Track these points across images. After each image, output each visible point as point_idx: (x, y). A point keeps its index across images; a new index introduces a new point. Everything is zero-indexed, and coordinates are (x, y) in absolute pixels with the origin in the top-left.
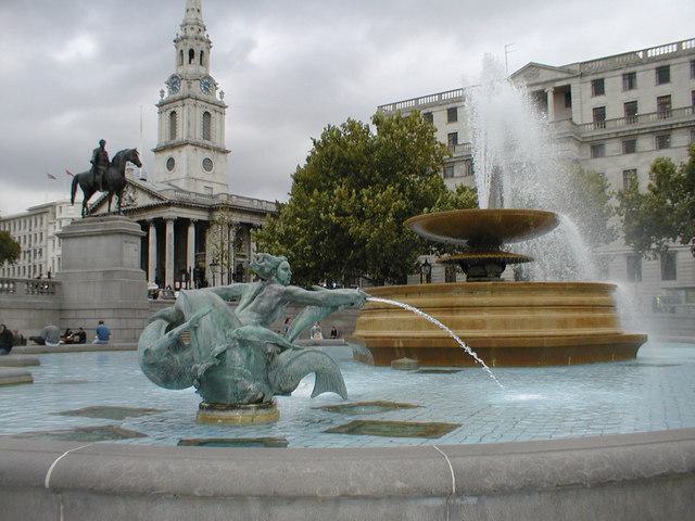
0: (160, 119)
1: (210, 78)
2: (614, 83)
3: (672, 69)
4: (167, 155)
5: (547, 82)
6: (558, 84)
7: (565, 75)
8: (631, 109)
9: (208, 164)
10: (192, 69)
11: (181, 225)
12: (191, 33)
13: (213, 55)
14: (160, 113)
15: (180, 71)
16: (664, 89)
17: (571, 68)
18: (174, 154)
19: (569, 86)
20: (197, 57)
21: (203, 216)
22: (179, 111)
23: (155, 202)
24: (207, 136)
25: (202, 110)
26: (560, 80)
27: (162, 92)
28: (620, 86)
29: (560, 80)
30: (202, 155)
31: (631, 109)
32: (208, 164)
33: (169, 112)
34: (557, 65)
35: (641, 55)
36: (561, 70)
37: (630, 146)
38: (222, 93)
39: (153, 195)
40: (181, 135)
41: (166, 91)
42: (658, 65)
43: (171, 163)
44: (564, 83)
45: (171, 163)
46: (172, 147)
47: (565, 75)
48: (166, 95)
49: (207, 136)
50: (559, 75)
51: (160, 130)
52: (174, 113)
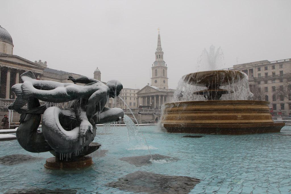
0: (152, 71)
1: (164, 62)
2: (263, 68)
3: (268, 67)
4: (155, 79)
5: (248, 68)
6: (250, 68)
7: (251, 67)
10: (160, 60)
11: (162, 96)
13: (164, 56)
14: (152, 69)
16: (266, 71)
19: (253, 69)
21: (165, 94)
22: (158, 69)
24: (164, 75)
25: (162, 69)
27: (153, 65)
30: (163, 79)
37: (266, 82)
38: (166, 65)
42: (273, 65)
43: (156, 82)
44: (251, 68)
45: (156, 82)
46: (157, 78)
47: (251, 67)
48: (154, 66)
49: (164, 75)
50: (250, 66)
51: (153, 73)
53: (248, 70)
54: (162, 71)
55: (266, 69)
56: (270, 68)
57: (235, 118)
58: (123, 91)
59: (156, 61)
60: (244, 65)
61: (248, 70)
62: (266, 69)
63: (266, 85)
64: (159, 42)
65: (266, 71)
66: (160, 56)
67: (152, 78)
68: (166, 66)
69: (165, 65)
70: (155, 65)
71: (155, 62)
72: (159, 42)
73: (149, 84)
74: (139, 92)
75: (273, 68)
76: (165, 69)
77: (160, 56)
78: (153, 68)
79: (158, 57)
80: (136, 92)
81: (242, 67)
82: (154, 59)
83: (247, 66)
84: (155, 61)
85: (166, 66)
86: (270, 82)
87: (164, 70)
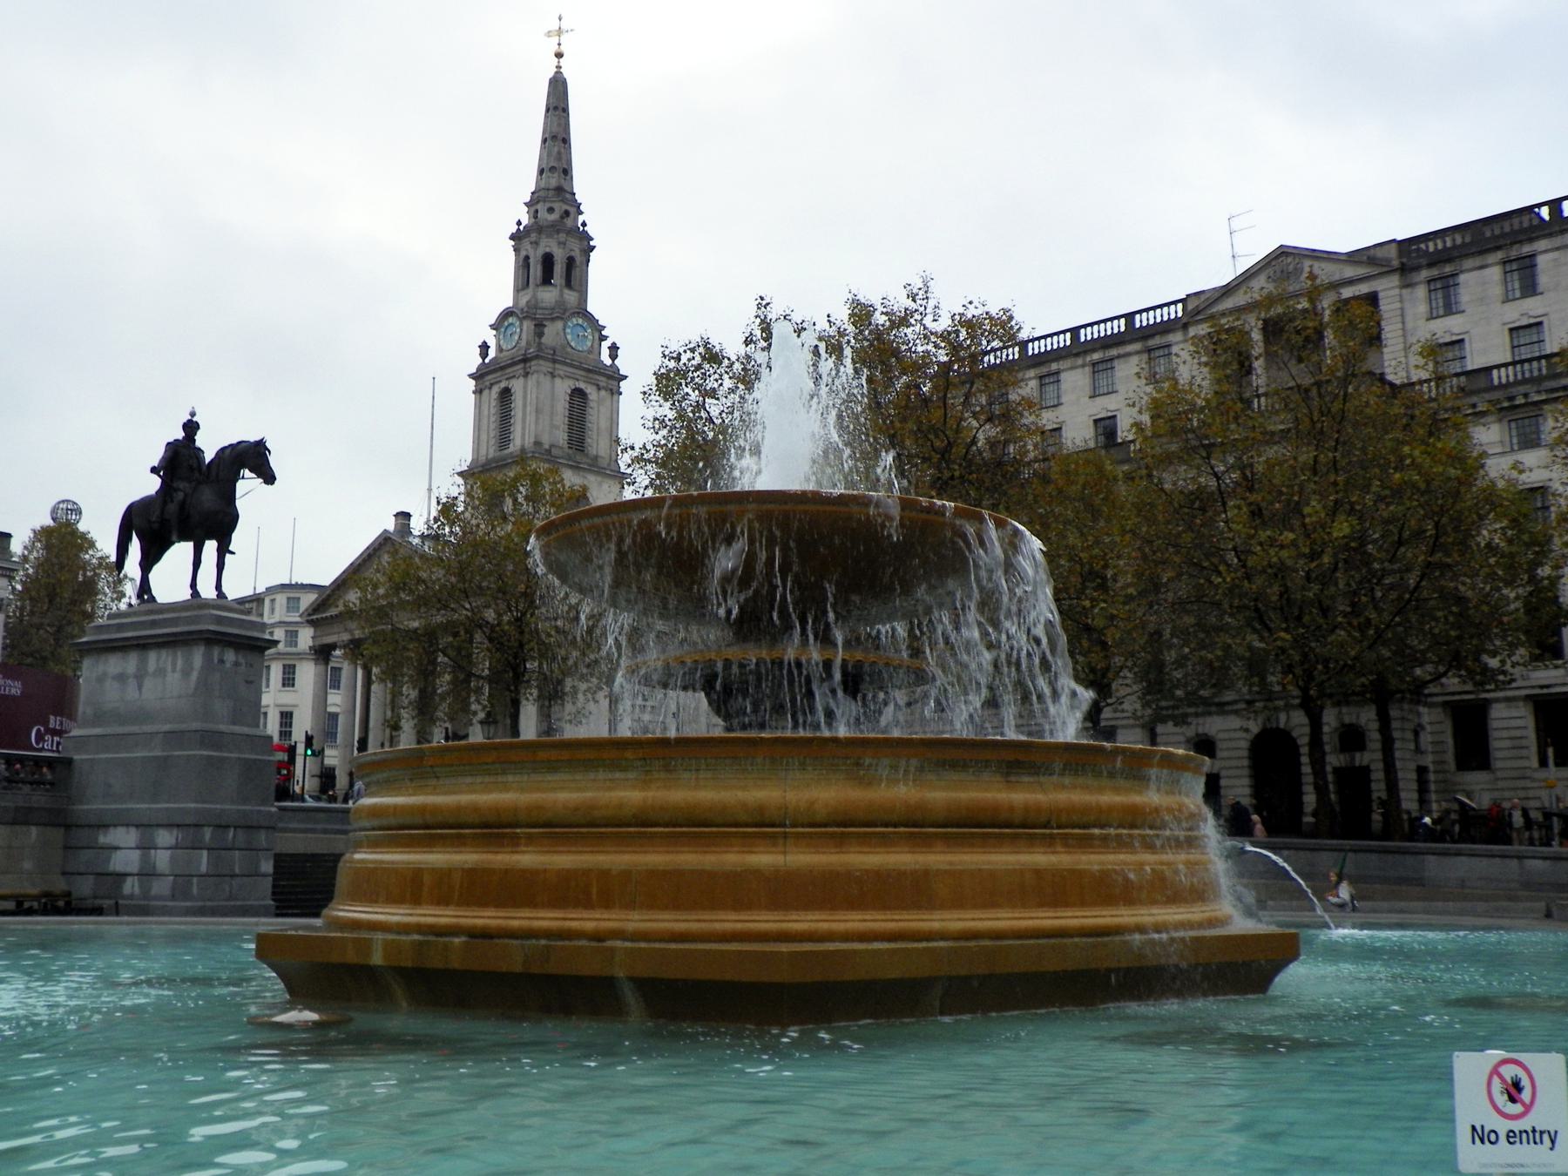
7: (1361, 271)
14: (478, 392)
17: (1379, 253)
20: (559, 269)
22: (517, 386)
25: (563, 387)
26: (1351, 282)
27: (484, 347)
28: (1497, 291)
29: (1351, 282)
33: (496, 389)
34: (1344, 246)
35: (1545, 212)
36: (1354, 257)
38: (614, 349)
41: (492, 343)
44: (1364, 289)
47: (1361, 271)
48: (492, 353)
50: (1350, 272)
52: (506, 394)
54: (562, 406)
57: (914, 891)
58: (273, 610)
59: (506, 314)
64: (557, 138)
66: (548, 261)
68: (614, 356)
69: (605, 358)
70: (500, 349)
72: (557, 138)
73: (404, 516)
74: (318, 607)
76: (590, 390)
77: (548, 261)
78: (478, 376)
79: (536, 271)
80: (308, 599)
85: (614, 356)
87: (578, 394)
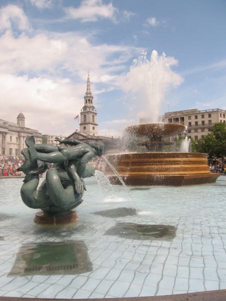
4: (84, 126)
8: (203, 122)
9: (94, 128)
10: (88, 105)
12: (89, 95)
15: (86, 105)
16: (196, 120)
18: (86, 126)
22: (87, 115)
23: (84, 138)
24: (93, 121)
25: (92, 115)
31: (203, 122)
32: (94, 128)
39: (84, 136)
40: (87, 121)
43: (85, 128)
46: (85, 124)
53: (179, 118)
55: (196, 117)
56: (199, 117)
60: (175, 113)
61: (179, 118)
62: (196, 117)
63: (196, 134)
65: (196, 120)
66: (89, 100)
67: (80, 125)
71: (85, 108)
75: (203, 117)
81: (173, 115)
82: (82, 103)
83: (178, 115)
84: (83, 105)
86: (199, 131)
